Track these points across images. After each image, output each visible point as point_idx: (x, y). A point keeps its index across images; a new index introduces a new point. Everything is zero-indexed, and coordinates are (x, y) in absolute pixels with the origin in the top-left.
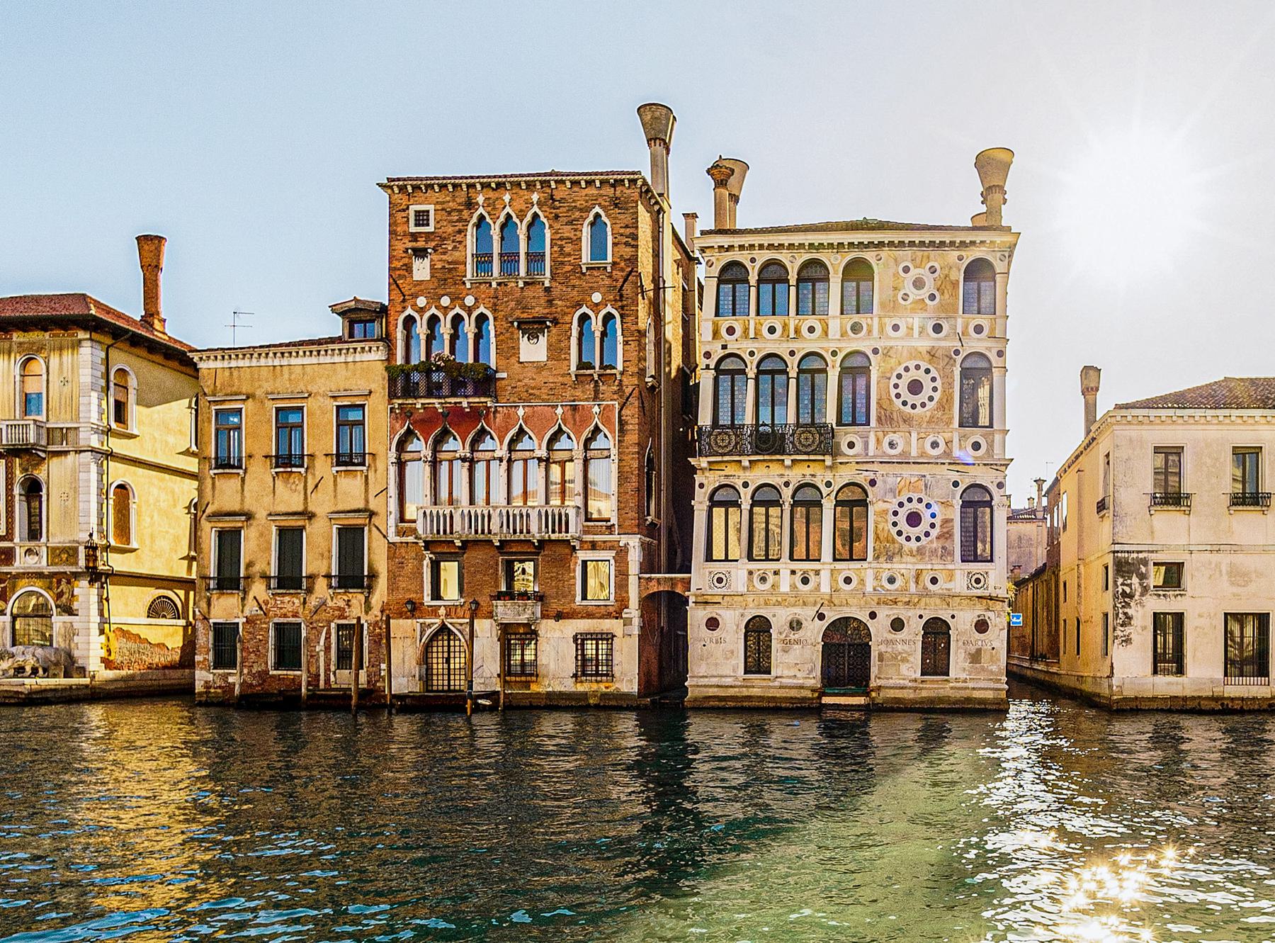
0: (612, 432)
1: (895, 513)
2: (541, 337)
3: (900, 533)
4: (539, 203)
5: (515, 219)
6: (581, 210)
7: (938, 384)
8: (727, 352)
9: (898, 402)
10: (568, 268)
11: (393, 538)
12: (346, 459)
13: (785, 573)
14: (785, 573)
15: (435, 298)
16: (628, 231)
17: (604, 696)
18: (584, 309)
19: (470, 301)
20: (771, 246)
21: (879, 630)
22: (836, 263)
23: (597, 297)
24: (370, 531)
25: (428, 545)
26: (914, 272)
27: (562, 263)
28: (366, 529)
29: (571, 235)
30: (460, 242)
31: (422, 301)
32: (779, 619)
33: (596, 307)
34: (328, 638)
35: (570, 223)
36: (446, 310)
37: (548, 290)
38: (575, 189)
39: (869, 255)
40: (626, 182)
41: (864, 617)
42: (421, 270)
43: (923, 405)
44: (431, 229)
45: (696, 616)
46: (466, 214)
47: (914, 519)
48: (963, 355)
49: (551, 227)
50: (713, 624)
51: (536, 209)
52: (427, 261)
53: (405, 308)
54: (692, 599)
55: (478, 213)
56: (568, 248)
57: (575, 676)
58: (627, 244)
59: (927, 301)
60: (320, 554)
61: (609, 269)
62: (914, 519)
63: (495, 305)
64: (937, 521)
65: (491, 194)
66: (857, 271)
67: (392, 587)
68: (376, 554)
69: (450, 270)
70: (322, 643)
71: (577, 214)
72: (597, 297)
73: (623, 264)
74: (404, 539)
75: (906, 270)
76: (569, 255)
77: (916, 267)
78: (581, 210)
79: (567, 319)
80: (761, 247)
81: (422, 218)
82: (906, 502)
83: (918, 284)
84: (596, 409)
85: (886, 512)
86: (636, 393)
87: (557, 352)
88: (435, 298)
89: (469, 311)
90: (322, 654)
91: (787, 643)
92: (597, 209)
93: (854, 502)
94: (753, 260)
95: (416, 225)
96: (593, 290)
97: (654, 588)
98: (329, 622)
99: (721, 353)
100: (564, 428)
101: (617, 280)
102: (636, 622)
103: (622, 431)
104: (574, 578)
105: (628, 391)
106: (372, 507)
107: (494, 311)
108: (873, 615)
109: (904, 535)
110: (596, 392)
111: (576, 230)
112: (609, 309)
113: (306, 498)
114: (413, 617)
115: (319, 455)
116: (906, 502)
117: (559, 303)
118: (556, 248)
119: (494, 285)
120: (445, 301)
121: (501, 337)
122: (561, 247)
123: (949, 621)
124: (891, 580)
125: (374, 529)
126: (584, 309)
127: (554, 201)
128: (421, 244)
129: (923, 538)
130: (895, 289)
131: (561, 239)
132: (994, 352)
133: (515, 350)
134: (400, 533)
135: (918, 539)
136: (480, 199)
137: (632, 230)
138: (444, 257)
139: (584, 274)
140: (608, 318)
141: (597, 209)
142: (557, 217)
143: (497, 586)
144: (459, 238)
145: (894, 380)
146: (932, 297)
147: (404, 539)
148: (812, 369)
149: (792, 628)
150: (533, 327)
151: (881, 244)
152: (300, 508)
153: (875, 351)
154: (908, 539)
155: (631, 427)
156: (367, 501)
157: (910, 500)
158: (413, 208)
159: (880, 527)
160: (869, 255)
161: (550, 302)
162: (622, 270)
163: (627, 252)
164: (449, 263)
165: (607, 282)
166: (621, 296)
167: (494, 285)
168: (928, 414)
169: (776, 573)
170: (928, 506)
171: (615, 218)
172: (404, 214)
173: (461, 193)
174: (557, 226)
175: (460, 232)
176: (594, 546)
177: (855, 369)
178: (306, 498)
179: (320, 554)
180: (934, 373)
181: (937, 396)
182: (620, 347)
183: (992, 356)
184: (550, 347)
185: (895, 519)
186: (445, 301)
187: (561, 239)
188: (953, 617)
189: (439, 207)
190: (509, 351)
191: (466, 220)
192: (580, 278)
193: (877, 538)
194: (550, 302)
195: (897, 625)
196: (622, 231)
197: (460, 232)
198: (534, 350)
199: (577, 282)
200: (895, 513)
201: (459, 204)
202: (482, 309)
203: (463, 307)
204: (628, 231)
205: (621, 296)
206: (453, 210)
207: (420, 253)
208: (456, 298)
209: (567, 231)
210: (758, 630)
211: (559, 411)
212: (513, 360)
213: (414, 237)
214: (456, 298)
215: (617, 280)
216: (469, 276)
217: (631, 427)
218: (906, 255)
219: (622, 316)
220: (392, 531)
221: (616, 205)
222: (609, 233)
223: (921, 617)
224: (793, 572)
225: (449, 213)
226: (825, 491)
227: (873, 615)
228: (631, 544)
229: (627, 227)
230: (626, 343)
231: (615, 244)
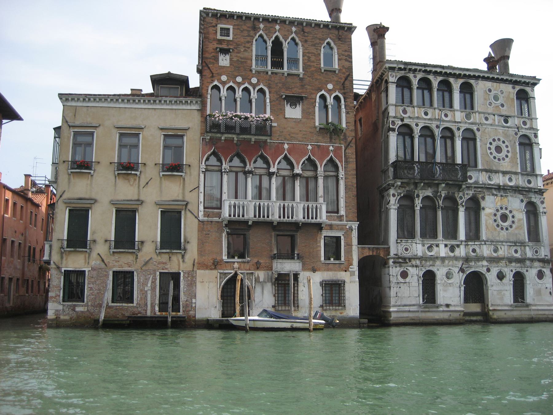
0: (341, 161)
1: (495, 215)
2: (298, 106)
3: (498, 226)
4: (295, 32)
5: (281, 39)
6: (320, 39)
7: (509, 149)
8: (404, 123)
9: (492, 157)
10: (313, 69)
11: (201, 217)
12: (174, 168)
13: (442, 246)
14: (442, 246)
15: (232, 77)
16: (346, 53)
17: (342, 319)
18: (323, 92)
19: (254, 80)
20: (425, 71)
21: (491, 277)
22: (456, 84)
23: (330, 86)
24: (185, 213)
25: (230, 223)
26: (493, 92)
27: (310, 66)
28: (183, 213)
29: (315, 51)
30: (249, 48)
31: (224, 78)
32: (440, 273)
33: (330, 92)
34: (154, 282)
35: (314, 45)
36: (239, 84)
37: (302, 79)
38: (316, 28)
39: (472, 81)
40: (346, 28)
41: (483, 270)
42: (224, 61)
43: (503, 159)
44: (231, 38)
45: (394, 271)
46: (252, 33)
47: (504, 218)
48: (519, 136)
49: (302, 46)
50: (404, 275)
51: (294, 35)
52: (228, 57)
53: (213, 81)
54: (391, 261)
55: (260, 33)
56: (313, 58)
57: (322, 306)
58: (346, 60)
59: (500, 107)
60: (149, 228)
61: (337, 72)
62: (504, 218)
63: (269, 84)
64: (516, 220)
65: (268, 25)
66: (467, 90)
67: (201, 252)
68: (189, 228)
69: (242, 62)
70: (149, 285)
71: (318, 41)
72: (330, 86)
73: (344, 70)
74: (210, 219)
75: (490, 91)
76: (313, 62)
77: (495, 90)
78: (320, 39)
79: (313, 96)
80: (420, 70)
81: (225, 31)
82: (500, 209)
83: (496, 98)
84: (331, 148)
85: (490, 214)
86: (354, 140)
87: (308, 114)
88: (232, 77)
89: (254, 86)
90: (149, 292)
91: (446, 285)
92: (329, 40)
93: (475, 208)
94: (415, 77)
95: (221, 35)
96: (328, 82)
97: (367, 253)
98: (155, 271)
99: (400, 123)
100: (312, 157)
101: (341, 79)
102: (357, 273)
103: (346, 162)
104: (320, 246)
105: (349, 139)
106: (187, 199)
107: (269, 88)
108: (488, 270)
109: (500, 227)
110: (331, 138)
111: (317, 49)
112: (337, 93)
113: (139, 192)
114: (215, 268)
115: (150, 164)
116: (500, 209)
117: (309, 87)
118: (306, 58)
119: (270, 73)
120: (239, 79)
121: (273, 103)
122: (309, 57)
123: (526, 273)
124: (496, 251)
125: (188, 212)
126: (323, 92)
127: (304, 32)
128: (224, 46)
129: (509, 228)
130: (485, 99)
131: (308, 53)
132: (533, 135)
133: (283, 111)
134: (206, 215)
135: (507, 229)
136: (262, 26)
137: (349, 53)
138: (238, 55)
139: (322, 73)
140: (337, 98)
141: (329, 40)
142: (306, 41)
143: (271, 251)
144: (248, 45)
145: (488, 145)
146: (502, 105)
147: (210, 219)
148: (448, 134)
149: (448, 278)
150: (294, 100)
151: (479, 77)
152: (136, 197)
153: (478, 130)
154: (502, 229)
155: (351, 160)
156: (183, 194)
157: (502, 208)
158: (220, 26)
159: (488, 222)
160: (472, 81)
161: (303, 86)
162: (344, 73)
163: (347, 64)
164: (241, 58)
165: (336, 79)
166: (344, 87)
167: (270, 73)
168: (506, 164)
169: (437, 246)
170: (511, 212)
171: (339, 46)
172: (213, 28)
173: (249, 22)
174: (306, 46)
175: (248, 42)
176: (331, 227)
177: (470, 139)
178: (139, 192)
179: (149, 228)
180: (507, 143)
181: (509, 155)
182: (344, 115)
183: (532, 137)
184: (303, 111)
185: (495, 218)
186: (239, 79)
187: (308, 53)
188: (527, 271)
189: (236, 27)
190: (278, 111)
191: (252, 36)
192: (320, 75)
193: (487, 228)
194: (303, 86)
195: (501, 276)
196: (343, 53)
197: (248, 42)
198: (294, 113)
199: (319, 77)
200: (495, 215)
201: (248, 27)
202: (261, 86)
203: (250, 84)
204: (346, 53)
205: (344, 87)
206: (244, 30)
207: (225, 51)
208: (246, 79)
209: (312, 49)
210: (429, 280)
211: (310, 147)
212: (281, 116)
213: (220, 42)
214: (246, 79)
215: (341, 79)
216: (254, 67)
217: (351, 160)
218: (489, 84)
219: (345, 98)
220: (201, 214)
221: (339, 39)
222: (336, 53)
223: (512, 271)
224: (446, 246)
225: (242, 31)
226: (460, 202)
227: (488, 270)
228: (354, 227)
229: (346, 51)
230: (347, 113)
231: (339, 60)
